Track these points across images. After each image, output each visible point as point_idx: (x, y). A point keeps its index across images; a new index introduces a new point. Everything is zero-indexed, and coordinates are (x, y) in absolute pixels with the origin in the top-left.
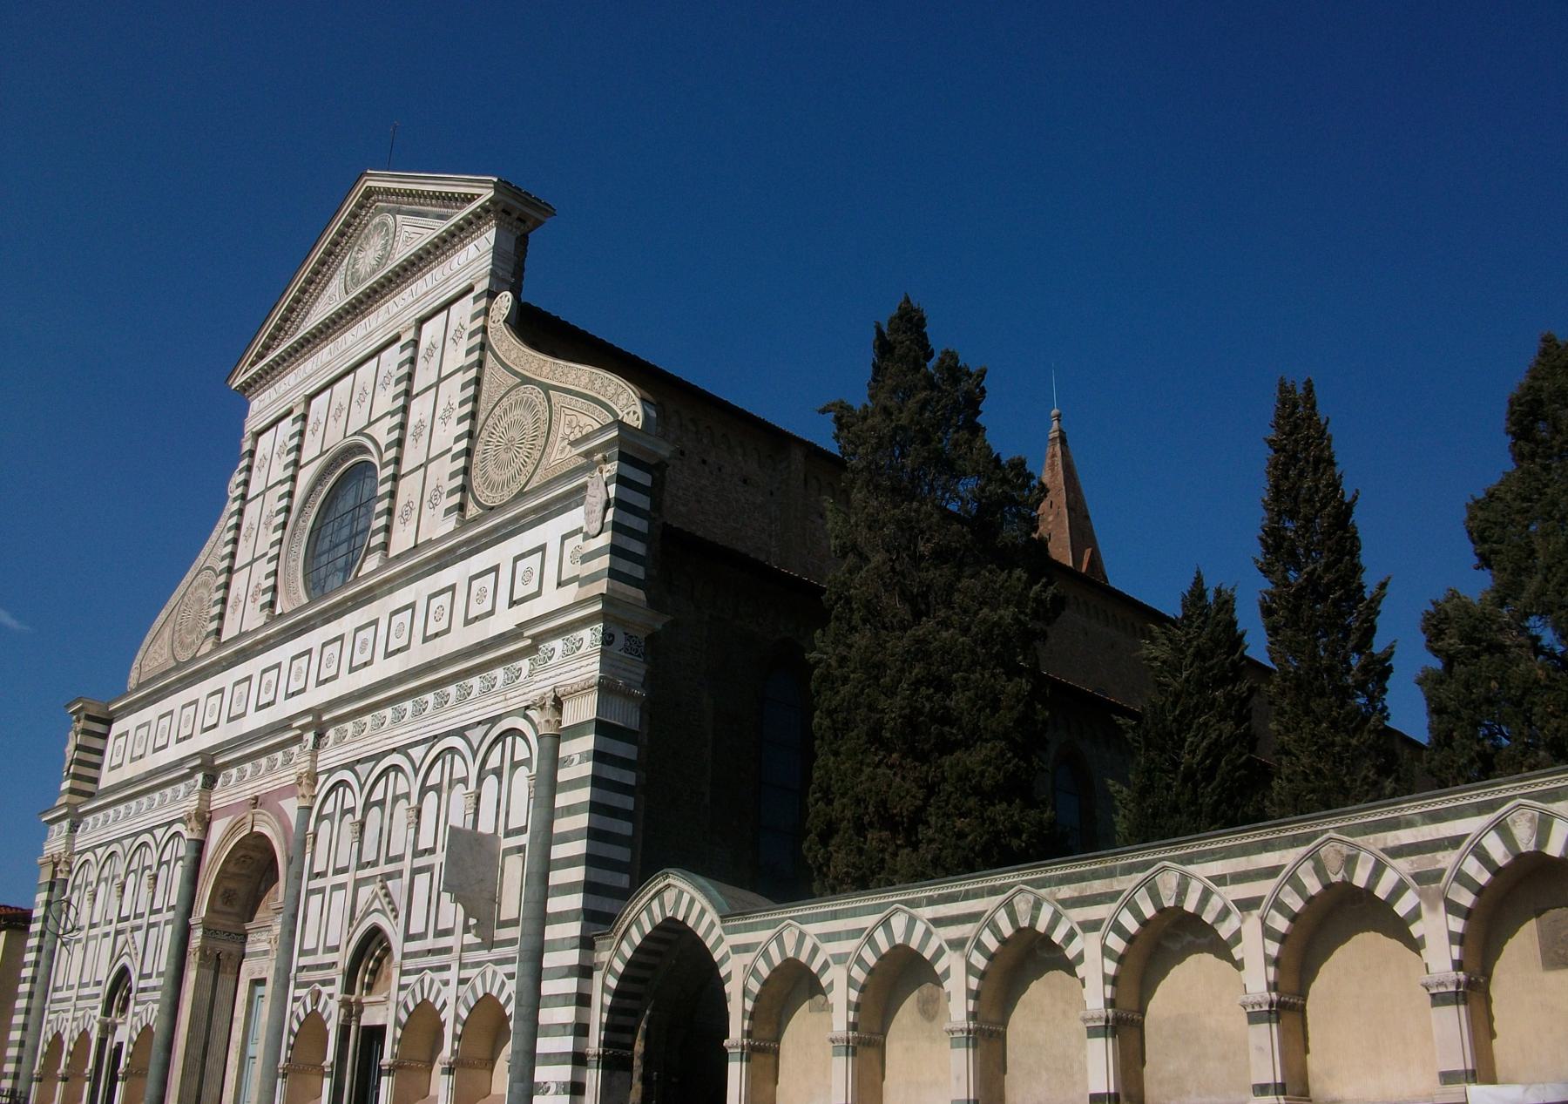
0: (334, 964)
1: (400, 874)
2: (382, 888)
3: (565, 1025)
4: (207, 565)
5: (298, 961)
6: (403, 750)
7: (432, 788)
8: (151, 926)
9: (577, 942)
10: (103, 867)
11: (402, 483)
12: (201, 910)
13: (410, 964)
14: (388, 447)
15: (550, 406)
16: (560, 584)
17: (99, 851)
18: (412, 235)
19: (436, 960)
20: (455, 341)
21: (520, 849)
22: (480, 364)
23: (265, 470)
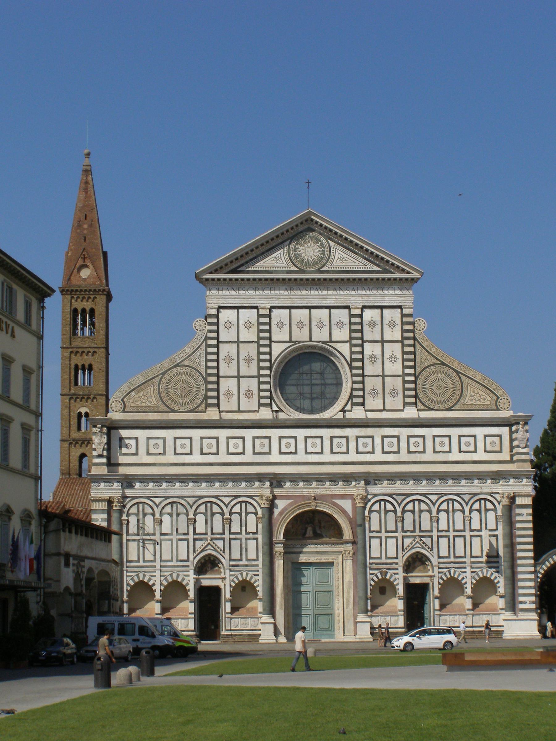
0: (397, 564)
1: (431, 537)
2: (420, 541)
3: (531, 587)
4: (186, 363)
5: (368, 561)
6: (424, 495)
7: (443, 510)
8: (231, 539)
9: (533, 565)
10: (163, 508)
11: (366, 378)
12: (279, 536)
13: (441, 566)
14: (353, 360)
15: (461, 380)
16: (485, 451)
17: (157, 501)
18: (345, 258)
19: (457, 565)
20: (390, 327)
21: (494, 536)
22: (414, 346)
23: (234, 330)
